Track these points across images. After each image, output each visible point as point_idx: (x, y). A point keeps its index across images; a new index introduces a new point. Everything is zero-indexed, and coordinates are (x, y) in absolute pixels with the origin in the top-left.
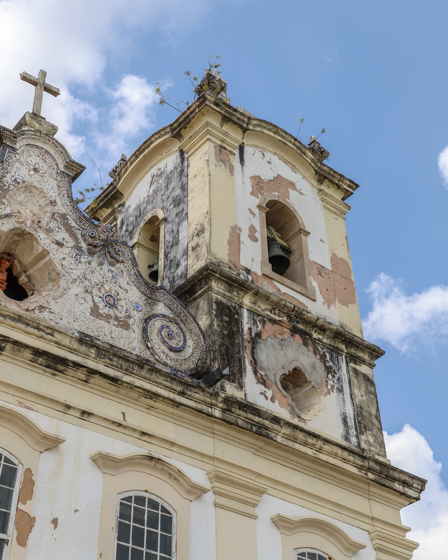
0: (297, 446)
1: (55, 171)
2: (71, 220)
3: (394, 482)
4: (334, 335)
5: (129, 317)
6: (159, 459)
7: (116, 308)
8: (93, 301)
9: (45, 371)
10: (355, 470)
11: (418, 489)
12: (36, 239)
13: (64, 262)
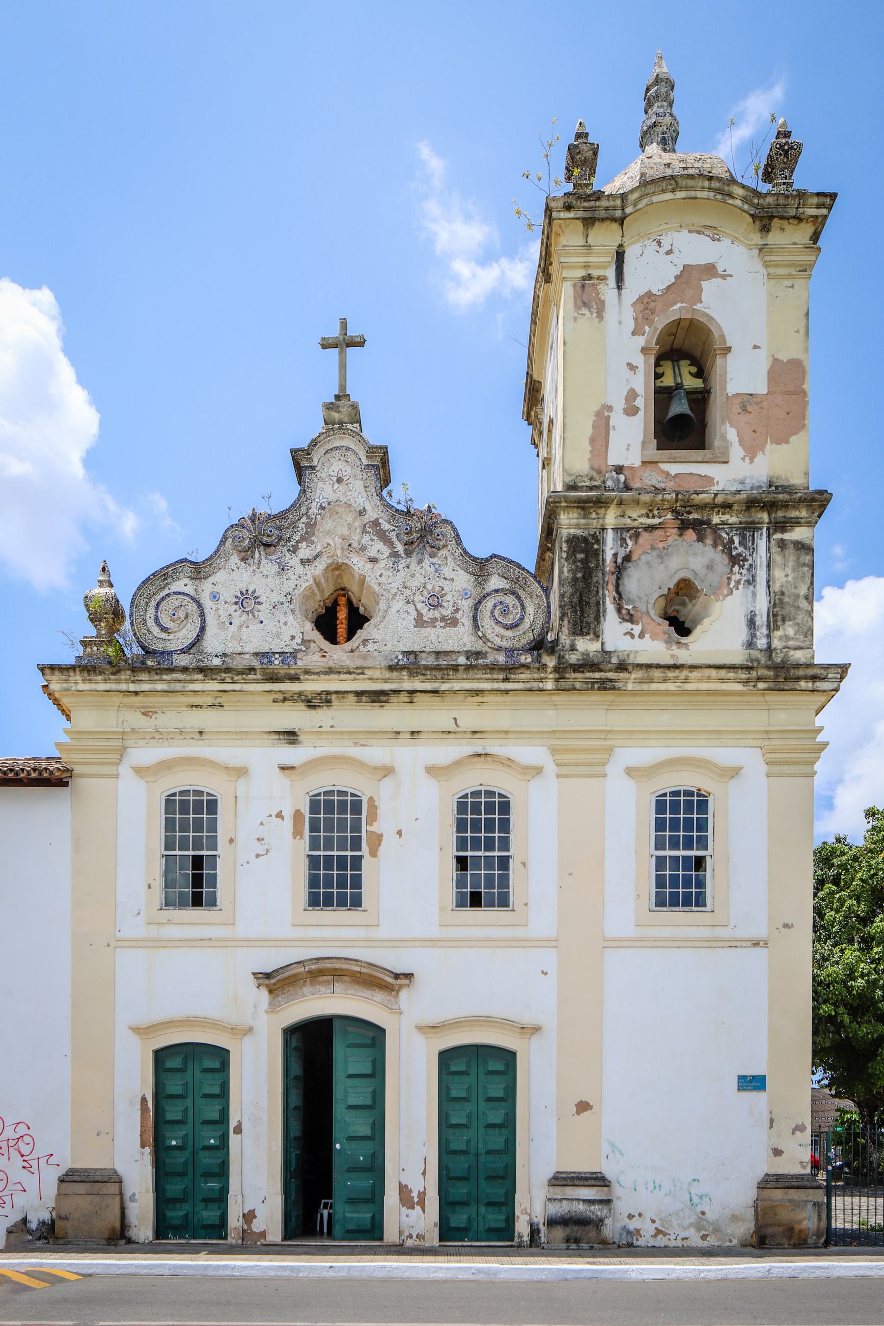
1: (359, 469)
2: (385, 523)
4: (747, 507)
5: (457, 610)
6: (486, 754)
7: (441, 606)
8: (416, 610)
9: (373, 706)
12: (351, 567)
13: (382, 580)
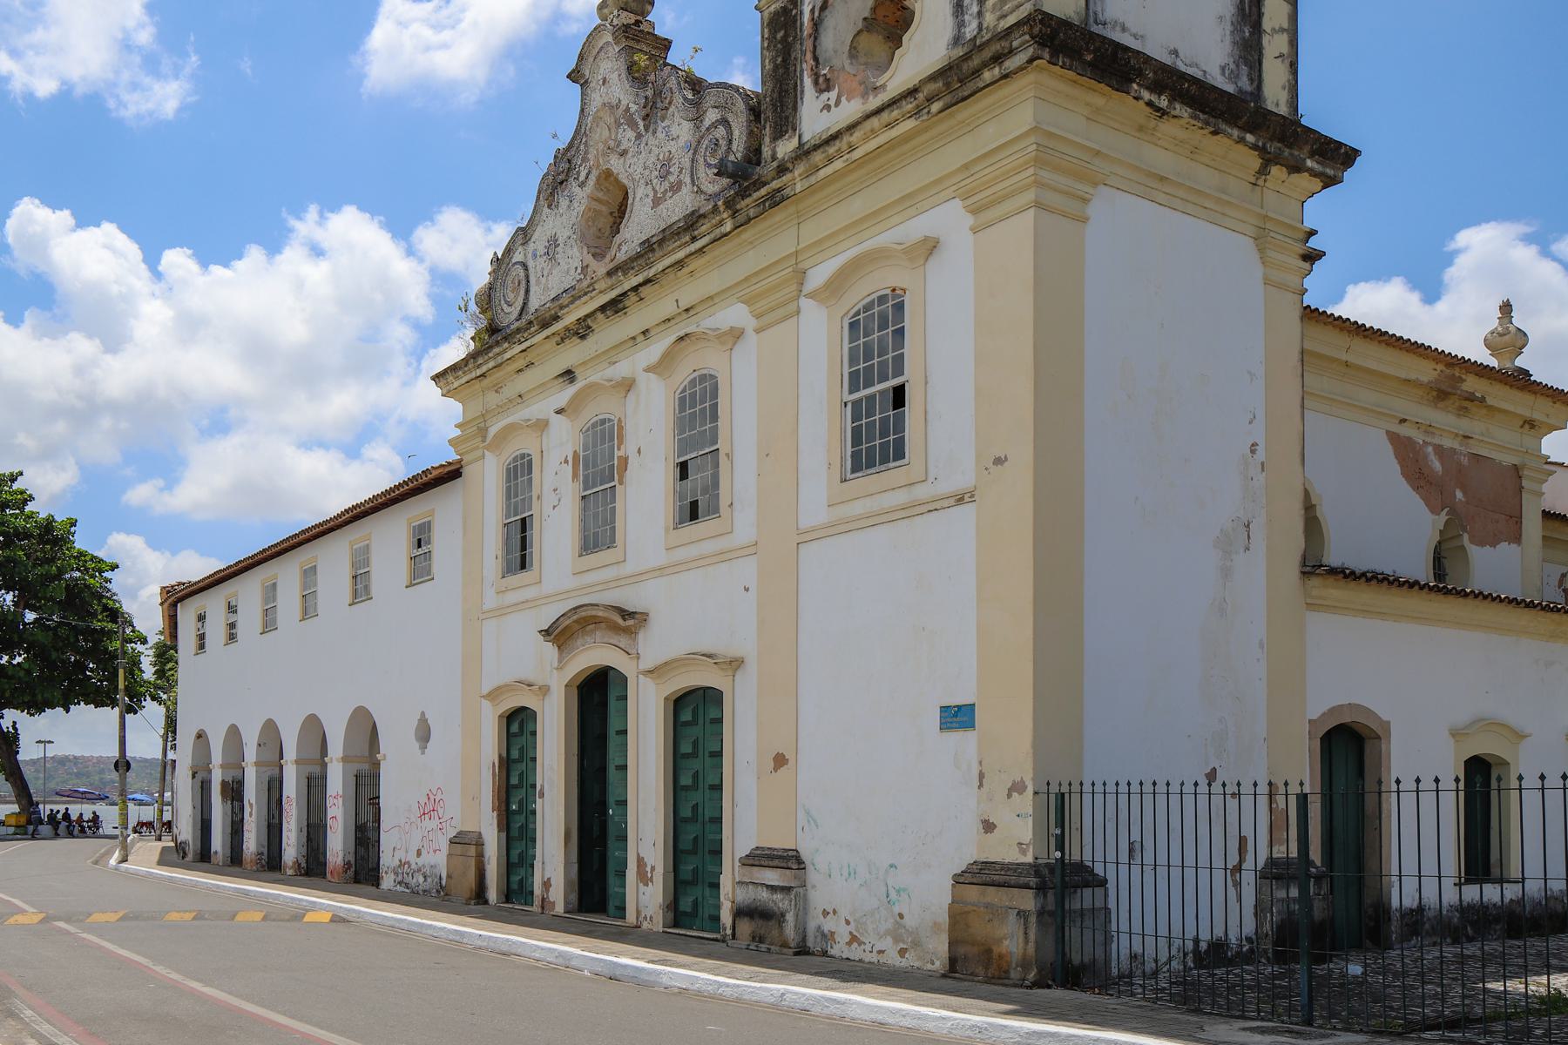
0: (822, 173)
3: (979, 75)
10: (910, 124)
11: (1028, 42)
